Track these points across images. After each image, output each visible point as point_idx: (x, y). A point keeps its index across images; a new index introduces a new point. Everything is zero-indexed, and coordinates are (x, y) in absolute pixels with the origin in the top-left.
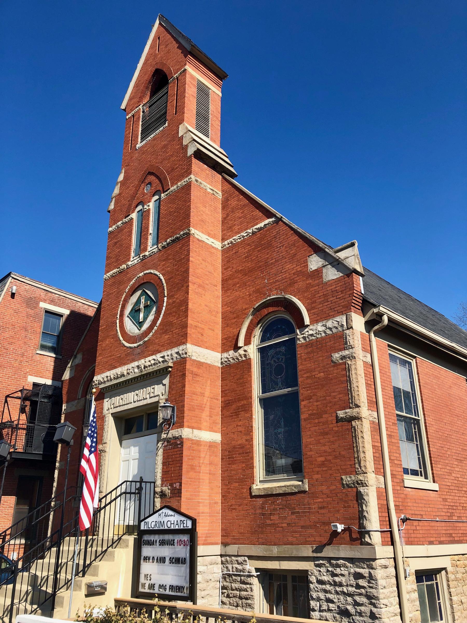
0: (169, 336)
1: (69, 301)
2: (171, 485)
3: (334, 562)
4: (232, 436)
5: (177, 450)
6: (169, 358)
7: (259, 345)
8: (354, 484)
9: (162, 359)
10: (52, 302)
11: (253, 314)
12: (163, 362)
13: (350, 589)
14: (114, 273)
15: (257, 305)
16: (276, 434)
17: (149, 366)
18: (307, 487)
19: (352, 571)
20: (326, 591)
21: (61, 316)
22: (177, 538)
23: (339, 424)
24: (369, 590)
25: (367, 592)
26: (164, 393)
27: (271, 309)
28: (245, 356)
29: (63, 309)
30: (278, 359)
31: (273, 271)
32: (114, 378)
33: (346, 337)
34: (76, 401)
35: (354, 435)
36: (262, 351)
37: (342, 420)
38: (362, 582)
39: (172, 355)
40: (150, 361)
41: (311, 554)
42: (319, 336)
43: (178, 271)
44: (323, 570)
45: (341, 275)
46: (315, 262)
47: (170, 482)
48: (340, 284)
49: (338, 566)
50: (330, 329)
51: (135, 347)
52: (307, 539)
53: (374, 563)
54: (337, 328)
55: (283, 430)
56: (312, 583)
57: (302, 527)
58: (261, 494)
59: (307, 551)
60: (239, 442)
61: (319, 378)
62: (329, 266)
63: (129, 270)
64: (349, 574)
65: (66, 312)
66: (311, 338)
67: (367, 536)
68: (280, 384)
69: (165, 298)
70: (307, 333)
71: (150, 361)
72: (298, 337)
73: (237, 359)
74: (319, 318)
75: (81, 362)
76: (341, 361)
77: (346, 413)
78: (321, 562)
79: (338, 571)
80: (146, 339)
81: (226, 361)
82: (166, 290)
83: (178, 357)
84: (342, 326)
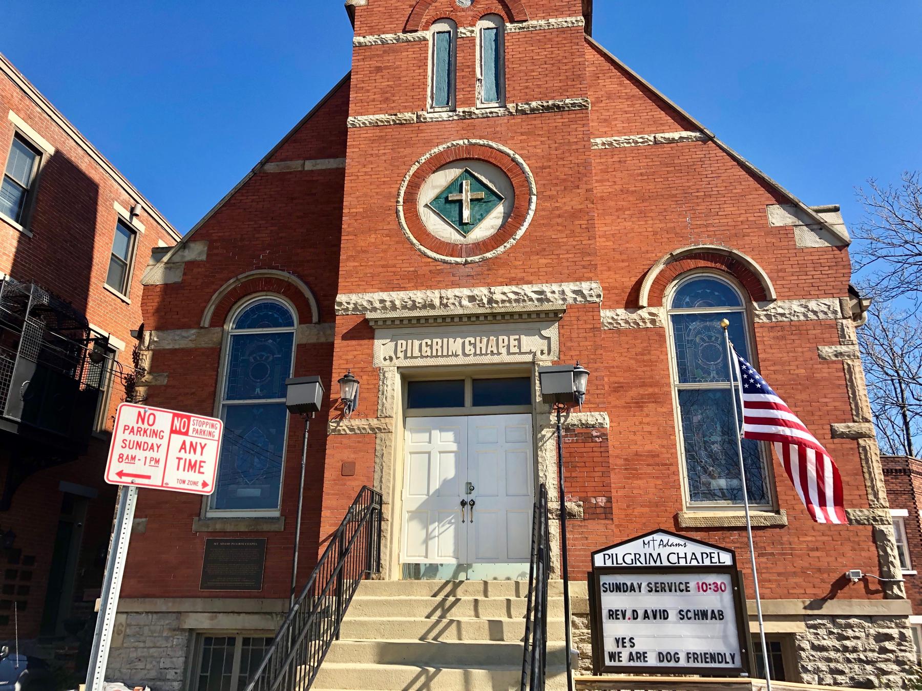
0: (549, 261)
1: (57, 129)
2: (585, 500)
3: (843, 621)
4: (632, 437)
5: (592, 445)
6: (556, 296)
7: (670, 311)
8: (868, 521)
9: (516, 297)
10: (28, 118)
11: (667, 263)
12: (517, 301)
13: (870, 654)
14: (382, 121)
15: (678, 251)
16: (705, 442)
17: (503, 301)
18: (785, 520)
19: (872, 631)
20: (829, 660)
21: (40, 154)
22: (693, 581)
23: (836, 441)
24: (901, 654)
25: (897, 657)
26: (546, 351)
27: (702, 263)
28: (653, 322)
29: (44, 140)
30: (710, 337)
31: (702, 208)
32: (404, 307)
33: (843, 330)
34: (193, 331)
35: (863, 457)
36: (676, 320)
37: (842, 435)
38: (889, 645)
39: (563, 292)
40: (504, 293)
41: (803, 612)
42: (795, 319)
43: (563, 159)
44: (822, 632)
45: (827, 244)
46: (778, 217)
47: (583, 495)
48: (826, 257)
49: (850, 626)
50: (815, 313)
51: (457, 263)
52: (791, 591)
53: (906, 621)
54: (825, 313)
55: (719, 439)
56: (803, 650)
57: (779, 574)
58: (699, 526)
59: (797, 607)
60: (648, 447)
61: (797, 375)
62: (805, 228)
63: (423, 126)
64: (868, 636)
65: (49, 149)
66: (780, 318)
67: (895, 587)
68: (714, 374)
69: (534, 198)
70: (773, 311)
71: (504, 293)
72: (757, 312)
73: (638, 324)
74: (792, 294)
75: (204, 257)
76: (834, 358)
77: (848, 427)
78: (820, 621)
79: (850, 633)
80: (489, 255)
81: (610, 323)
82: (533, 183)
83: (579, 299)
84: (835, 312)
